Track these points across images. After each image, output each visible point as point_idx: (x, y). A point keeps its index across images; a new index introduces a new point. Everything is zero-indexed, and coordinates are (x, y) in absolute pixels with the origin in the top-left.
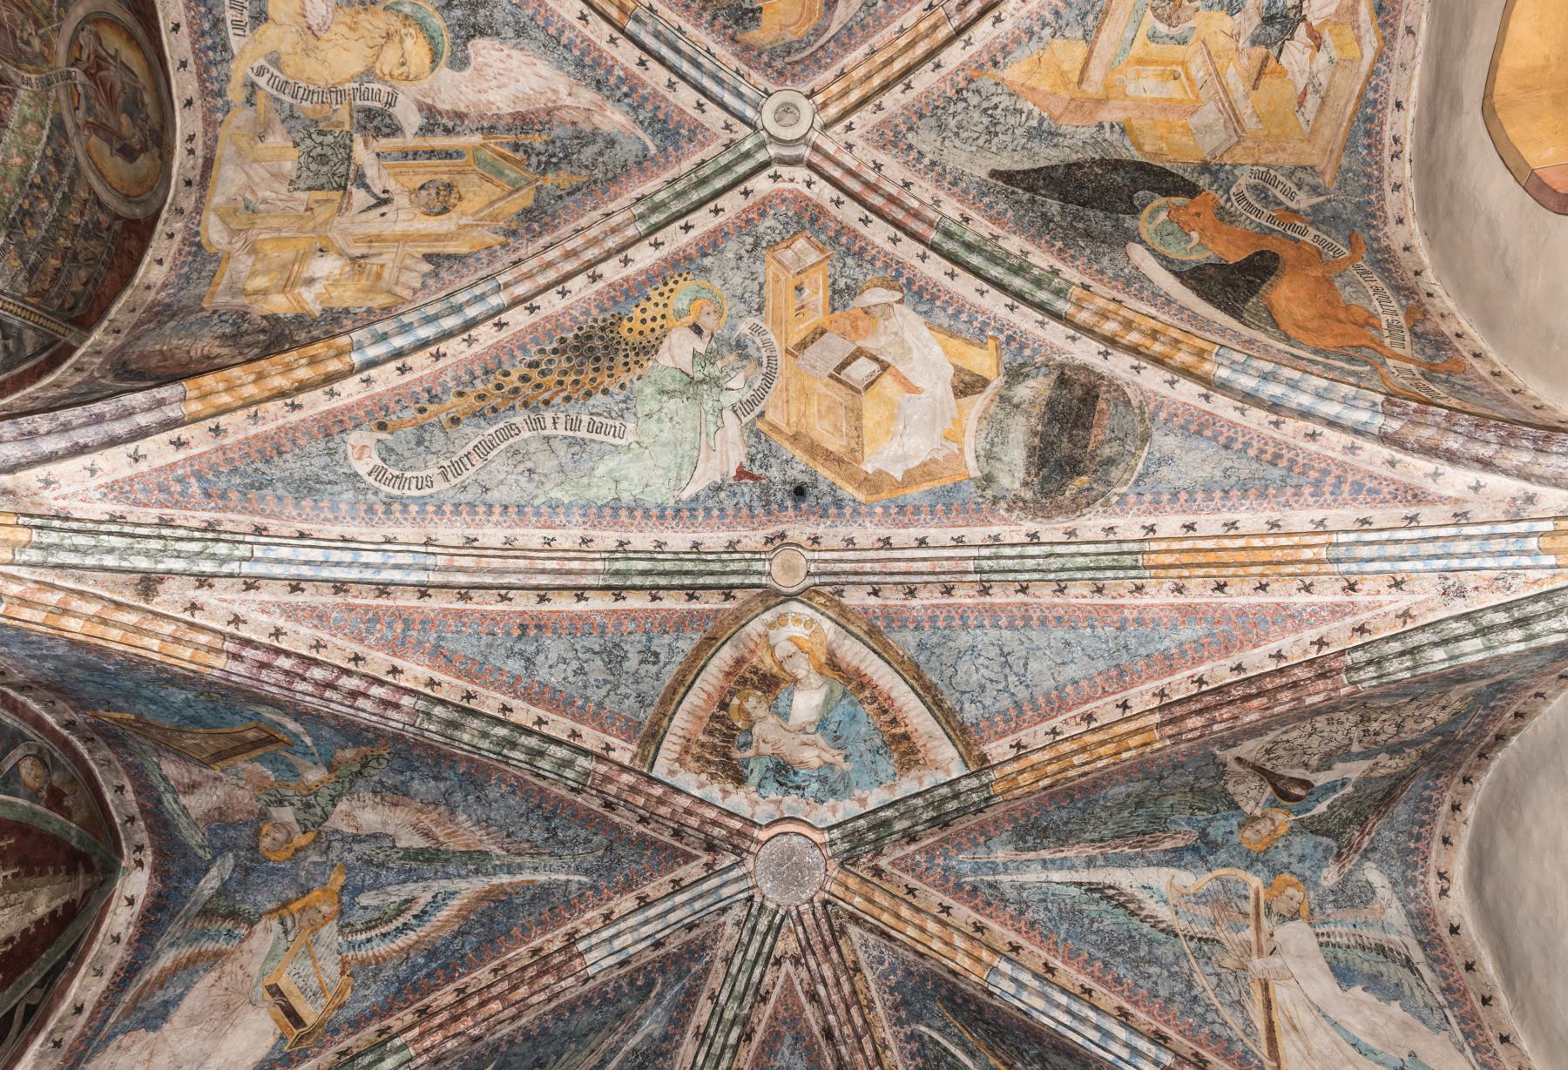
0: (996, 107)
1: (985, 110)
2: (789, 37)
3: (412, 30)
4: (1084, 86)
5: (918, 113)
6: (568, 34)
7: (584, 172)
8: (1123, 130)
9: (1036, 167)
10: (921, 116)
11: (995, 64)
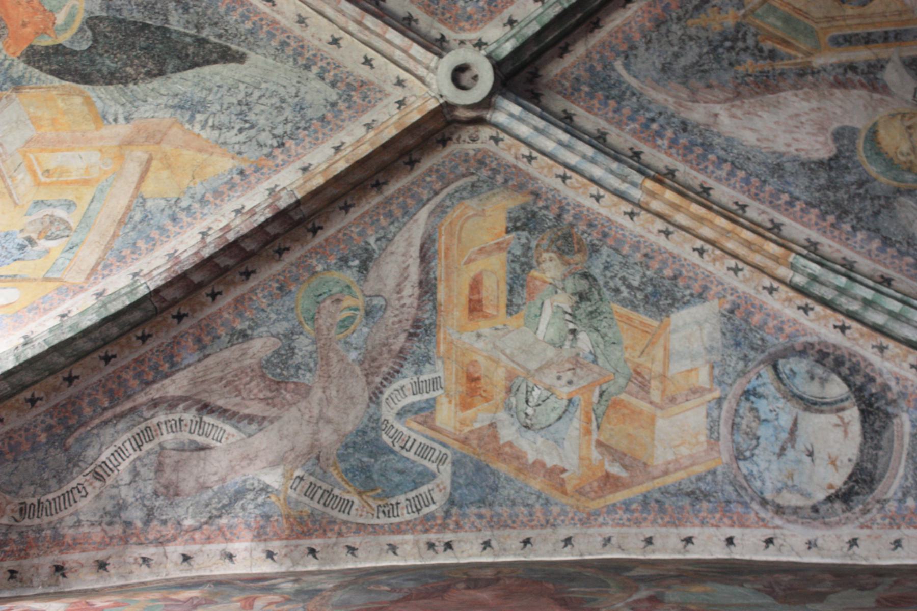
0: (241, 131)
1: (252, 127)
2: (473, 203)
3: (903, 159)
4: (145, 157)
5: (327, 121)
6: (723, 173)
7: (693, 31)
8: (104, 117)
9: (197, 69)
10: (323, 119)
11: (242, 173)
